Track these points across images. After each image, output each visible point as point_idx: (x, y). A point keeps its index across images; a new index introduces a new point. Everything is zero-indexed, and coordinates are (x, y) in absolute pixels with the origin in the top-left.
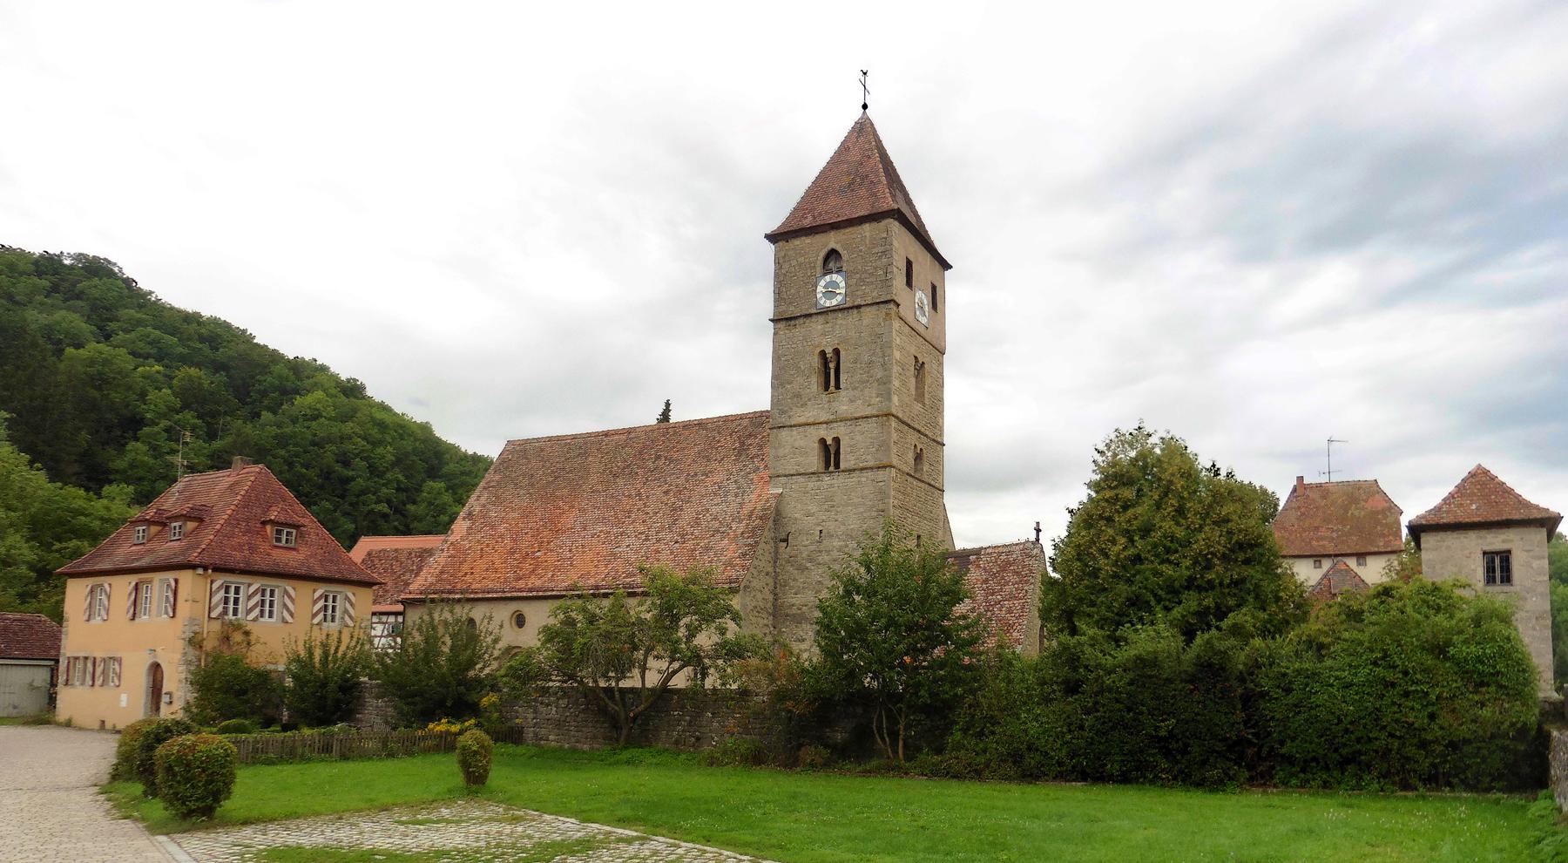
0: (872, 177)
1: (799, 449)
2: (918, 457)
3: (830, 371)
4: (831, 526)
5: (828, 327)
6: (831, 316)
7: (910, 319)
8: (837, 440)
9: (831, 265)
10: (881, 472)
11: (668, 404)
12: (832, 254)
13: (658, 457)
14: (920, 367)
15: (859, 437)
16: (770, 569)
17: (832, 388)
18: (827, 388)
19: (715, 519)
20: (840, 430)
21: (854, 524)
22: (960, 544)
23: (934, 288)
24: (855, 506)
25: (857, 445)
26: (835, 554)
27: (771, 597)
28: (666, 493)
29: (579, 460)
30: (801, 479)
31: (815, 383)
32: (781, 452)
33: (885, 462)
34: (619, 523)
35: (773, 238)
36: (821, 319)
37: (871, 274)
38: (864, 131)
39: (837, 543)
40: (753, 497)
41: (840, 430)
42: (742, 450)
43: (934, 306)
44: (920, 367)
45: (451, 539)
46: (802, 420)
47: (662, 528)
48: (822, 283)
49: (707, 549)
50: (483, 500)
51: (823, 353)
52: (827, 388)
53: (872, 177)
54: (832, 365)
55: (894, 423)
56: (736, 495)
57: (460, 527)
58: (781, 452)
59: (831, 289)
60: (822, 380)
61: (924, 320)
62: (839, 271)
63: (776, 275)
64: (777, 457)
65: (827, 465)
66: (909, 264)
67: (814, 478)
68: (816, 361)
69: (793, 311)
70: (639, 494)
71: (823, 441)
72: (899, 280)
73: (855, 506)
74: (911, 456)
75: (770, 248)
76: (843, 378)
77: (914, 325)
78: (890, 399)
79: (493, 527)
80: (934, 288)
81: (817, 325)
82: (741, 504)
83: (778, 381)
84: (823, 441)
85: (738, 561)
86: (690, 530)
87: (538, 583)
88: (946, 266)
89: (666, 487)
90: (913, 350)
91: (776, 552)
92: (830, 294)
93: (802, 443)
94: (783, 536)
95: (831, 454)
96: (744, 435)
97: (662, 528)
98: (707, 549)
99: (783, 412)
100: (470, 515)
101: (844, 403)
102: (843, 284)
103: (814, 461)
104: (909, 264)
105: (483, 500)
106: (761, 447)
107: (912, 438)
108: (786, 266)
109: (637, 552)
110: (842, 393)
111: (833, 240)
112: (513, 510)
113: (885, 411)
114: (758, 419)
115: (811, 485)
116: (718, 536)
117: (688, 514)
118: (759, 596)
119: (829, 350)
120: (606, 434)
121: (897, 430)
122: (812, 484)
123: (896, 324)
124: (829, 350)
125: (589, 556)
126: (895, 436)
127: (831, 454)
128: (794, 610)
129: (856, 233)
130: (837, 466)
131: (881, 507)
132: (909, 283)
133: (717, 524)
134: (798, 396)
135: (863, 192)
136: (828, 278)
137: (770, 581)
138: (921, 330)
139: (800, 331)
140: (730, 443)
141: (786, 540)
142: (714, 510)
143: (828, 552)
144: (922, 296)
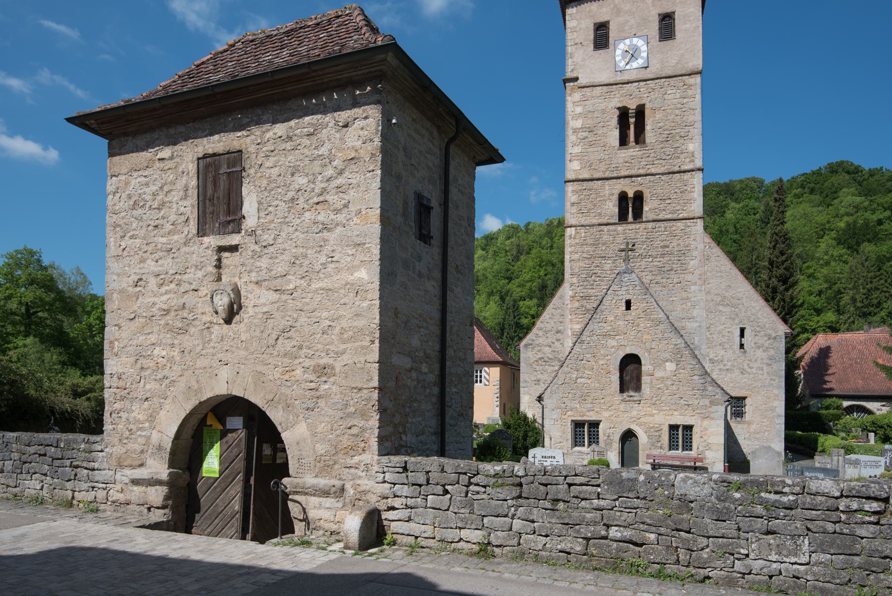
77: (620, 78)
118: (547, 348)
138: (633, 76)
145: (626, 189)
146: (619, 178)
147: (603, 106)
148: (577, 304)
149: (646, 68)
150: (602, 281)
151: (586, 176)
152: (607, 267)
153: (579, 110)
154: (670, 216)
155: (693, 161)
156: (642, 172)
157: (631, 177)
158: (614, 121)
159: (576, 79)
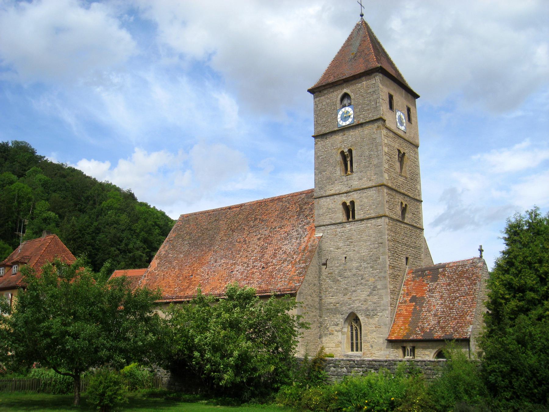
0: (366, 51)
1: (330, 209)
2: (404, 210)
4: (351, 254)
7: (393, 127)
8: (352, 203)
10: (379, 220)
13: (256, 219)
14: (402, 157)
15: (365, 200)
16: (316, 282)
17: (349, 172)
19: (285, 253)
20: (355, 196)
21: (364, 252)
22: (436, 261)
23: (409, 110)
24: (366, 241)
25: (365, 204)
26: (354, 271)
27: (317, 299)
28: (259, 239)
29: (215, 223)
30: (333, 227)
31: (339, 171)
32: (321, 212)
33: (381, 214)
34: (233, 258)
35: (311, 91)
37: (368, 105)
39: (355, 264)
40: (306, 239)
41: (355, 196)
42: (301, 211)
43: (409, 120)
44: (402, 157)
45: (149, 269)
46: (332, 192)
47: (256, 260)
48: (341, 113)
49: (279, 271)
50: (166, 248)
51: (342, 153)
52: (346, 173)
53: (366, 51)
54: (349, 159)
55: (385, 190)
56: (297, 239)
57: (155, 262)
58: (321, 212)
59: (345, 115)
60: (344, 167)
61: (403, 128)
62: (350, 105)
63: (315, 111)
64: (319, 215)
65: (348, 217)
66: (391, 97)
67: (340, 226)
68: (339, 158)
69: (325, 130)
70: (245, 241)
71: (344, 204)
72: (385, 107)
73: (366, 241)
74: (398, 210)
75: (311, 96)
76: (355, 165)
78: (382, 176)
79: (170, 263)
80: (409, 110)
81: (338, 138)
82: (299, 244)
83: (319, 170)
84: (344, 204)
85: (296, 277)
86: (271, 260)
87: (190, 293)
88: (416, 96)
89: (259, 237)
90: (397, 146)
91: (320, 271)
92: (345, 118)
93: (332, 206)
94: (324, 261)
95: (349, 210)
96: (301, 205)
97: (256, 260)
98: (279, 271)
99: (321, 188)
100: (160, 257)
101: (355, 181)
102: (352, 112)
103: (341, 216)
104: (391, 97)
105: (166, 248)
106: (311, 210)
107: (399, 199)
108: (320, 106)
109: (242, 274)
110: (354, 175)
112: (181, 253)
113: (380, 183)
114: (309, 194)
115: (339, 230)
116: (286, 264)
117: (270, 251)
118: (309, 297)
119: (346, 150)
120: (230, 208)
121: (388, 194)
122: (339, 229)
123: (384, 132)
124: (346, 150)
125: (217, 276)
126: (387, 198)
127: (349, 210)
128: (332, 306)
130: (353, 217)
131: (380, 241)
132: (391, 107)
133: (284, 256)
134: (329, 178)
135: (361, 60)
136: (343, 110)
137: (316, 289)
138: (401, 134)
140: (295, 208)
141: (325, 264)
142: (284, 248)
143: (350, 270)
144: (400, 114)
145: (403, 201)
146: (400, 193)
147: (393, 144)
148: (391, 271)
149: (405, 133)
150: (398, 257)
151: (390, 185)
152: (400, 249)
153: (386, 141)
154: (415, 224)
155: (419, 195)
156: (406, 193)
157: (403, 194)
158: (397, 157)
159: (384, 121)
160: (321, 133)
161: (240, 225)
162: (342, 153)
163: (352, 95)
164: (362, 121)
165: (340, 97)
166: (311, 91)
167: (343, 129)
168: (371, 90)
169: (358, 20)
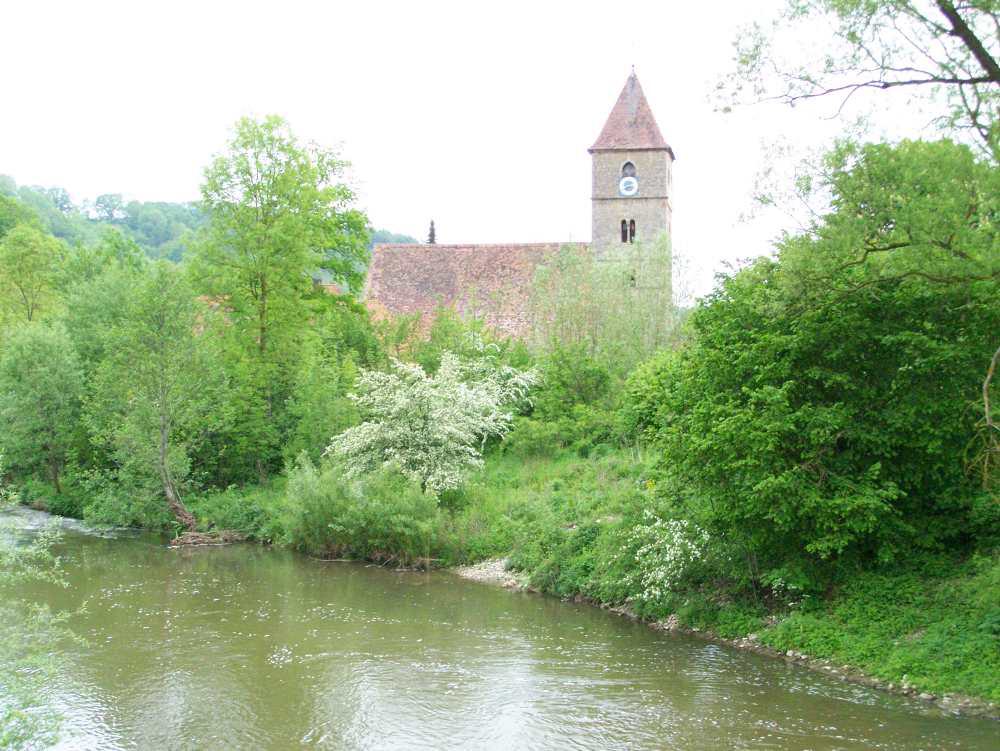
3: (627, 231)
5: (627, 207)
6: (629, 202)
9: (627, 171)
11: (432, 224)
12: (629, 164)
18: (624, 239)
31: (620, 239)
35: (591, 151)
36: (622, 202)
38: (633, 81)
51: (624, 222)
59: (629, 186)
62: (633, 175)
63: (594, 173)
69: (603, 194)
81: (620, 205)
111: (629, 158)
119: (628, 221)
124: (628, 221)
129: (631, 146)
139: (609, 207)
160: (600, 197)
161: (484, 272)
162: (624, 222)
163: (637, 167)
164: (646, 195)
165: (624, 163)
166: (591, 151)
167: (626, 199)
168: (658, 167)
169: (629, 74)
